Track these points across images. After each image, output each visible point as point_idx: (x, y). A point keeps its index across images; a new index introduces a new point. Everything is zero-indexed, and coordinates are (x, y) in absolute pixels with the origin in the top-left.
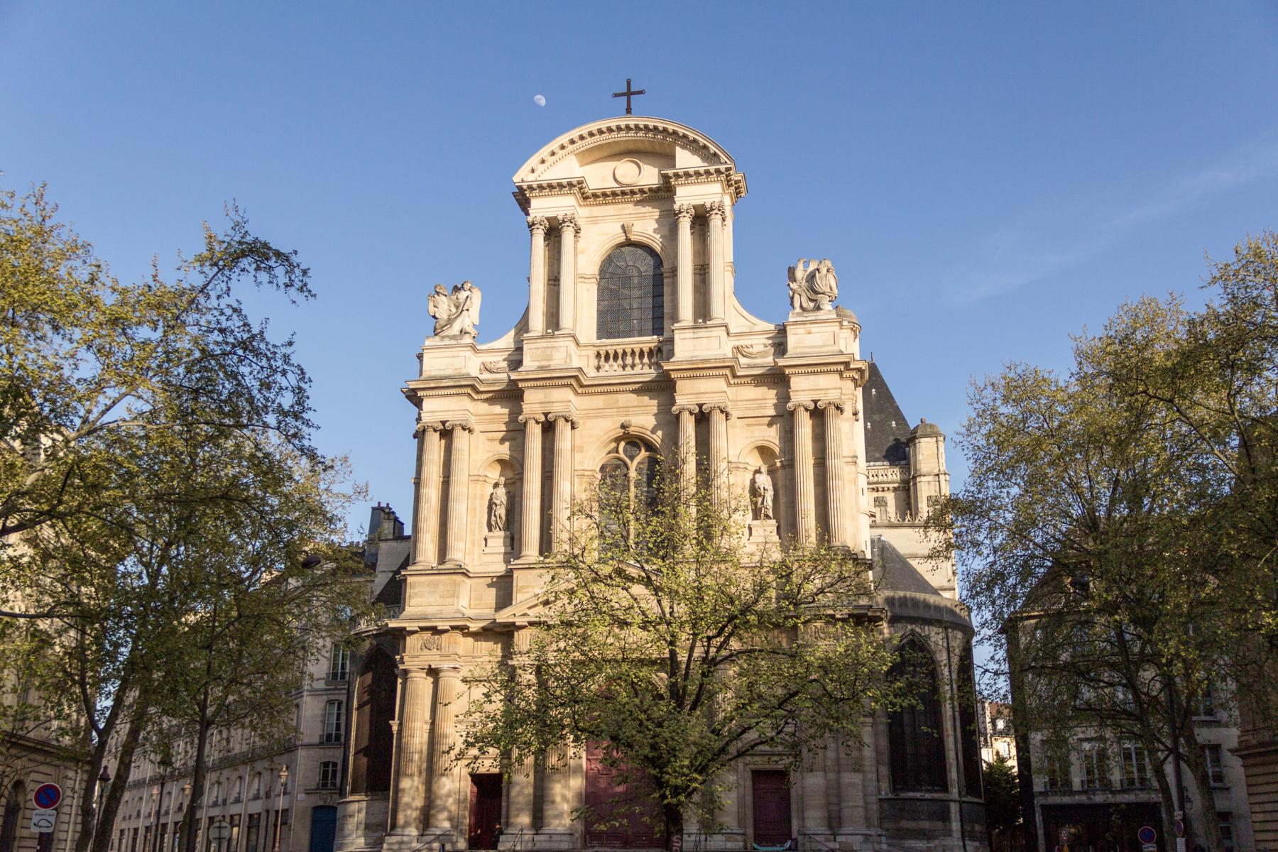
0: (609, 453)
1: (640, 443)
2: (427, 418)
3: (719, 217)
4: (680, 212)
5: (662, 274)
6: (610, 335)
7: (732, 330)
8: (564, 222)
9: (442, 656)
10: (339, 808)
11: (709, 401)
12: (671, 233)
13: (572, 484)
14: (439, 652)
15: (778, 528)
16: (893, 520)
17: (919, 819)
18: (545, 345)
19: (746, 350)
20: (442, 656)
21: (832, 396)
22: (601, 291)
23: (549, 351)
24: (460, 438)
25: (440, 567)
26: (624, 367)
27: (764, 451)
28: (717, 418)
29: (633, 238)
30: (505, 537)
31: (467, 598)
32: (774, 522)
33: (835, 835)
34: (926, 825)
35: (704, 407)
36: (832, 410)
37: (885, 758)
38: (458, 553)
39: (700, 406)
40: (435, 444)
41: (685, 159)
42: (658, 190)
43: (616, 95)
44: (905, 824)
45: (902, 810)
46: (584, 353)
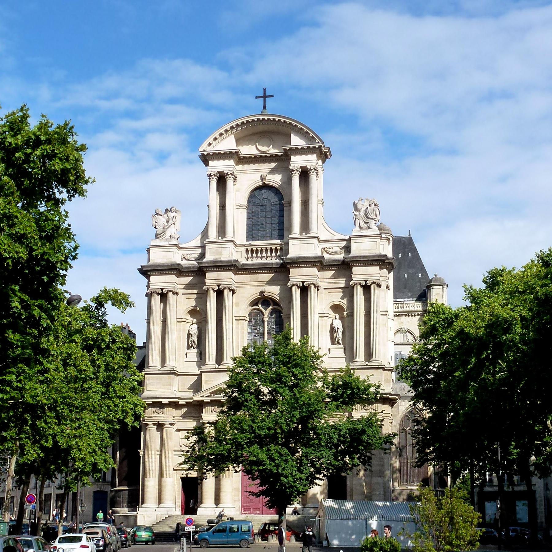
1: (270, 301)
2: (152, 286)
3: (315, 173)
4: (293, 170)
7: (322, 238)
9: (165, 417)
11: (308, 280)
12: (288, 181)
13: (233, 324)
14: (163, 415)
15: (345, 349)
16: (410, 341)
19: (329, 250)
21: (375, 278)
22: (249, 213)
23: (220, 249)
25: (162, 369)
26: (261, 258)
27: (336, 308)
28: (312, 290)
29: (266, 183)
30: (197, 353)
31: (177, 386)
35: (305, 283)
36: (374, 286)
38: (171, 363)
39: (303, 282)
40: (156, 299)
41: (296, 141)
46: (239, 250)
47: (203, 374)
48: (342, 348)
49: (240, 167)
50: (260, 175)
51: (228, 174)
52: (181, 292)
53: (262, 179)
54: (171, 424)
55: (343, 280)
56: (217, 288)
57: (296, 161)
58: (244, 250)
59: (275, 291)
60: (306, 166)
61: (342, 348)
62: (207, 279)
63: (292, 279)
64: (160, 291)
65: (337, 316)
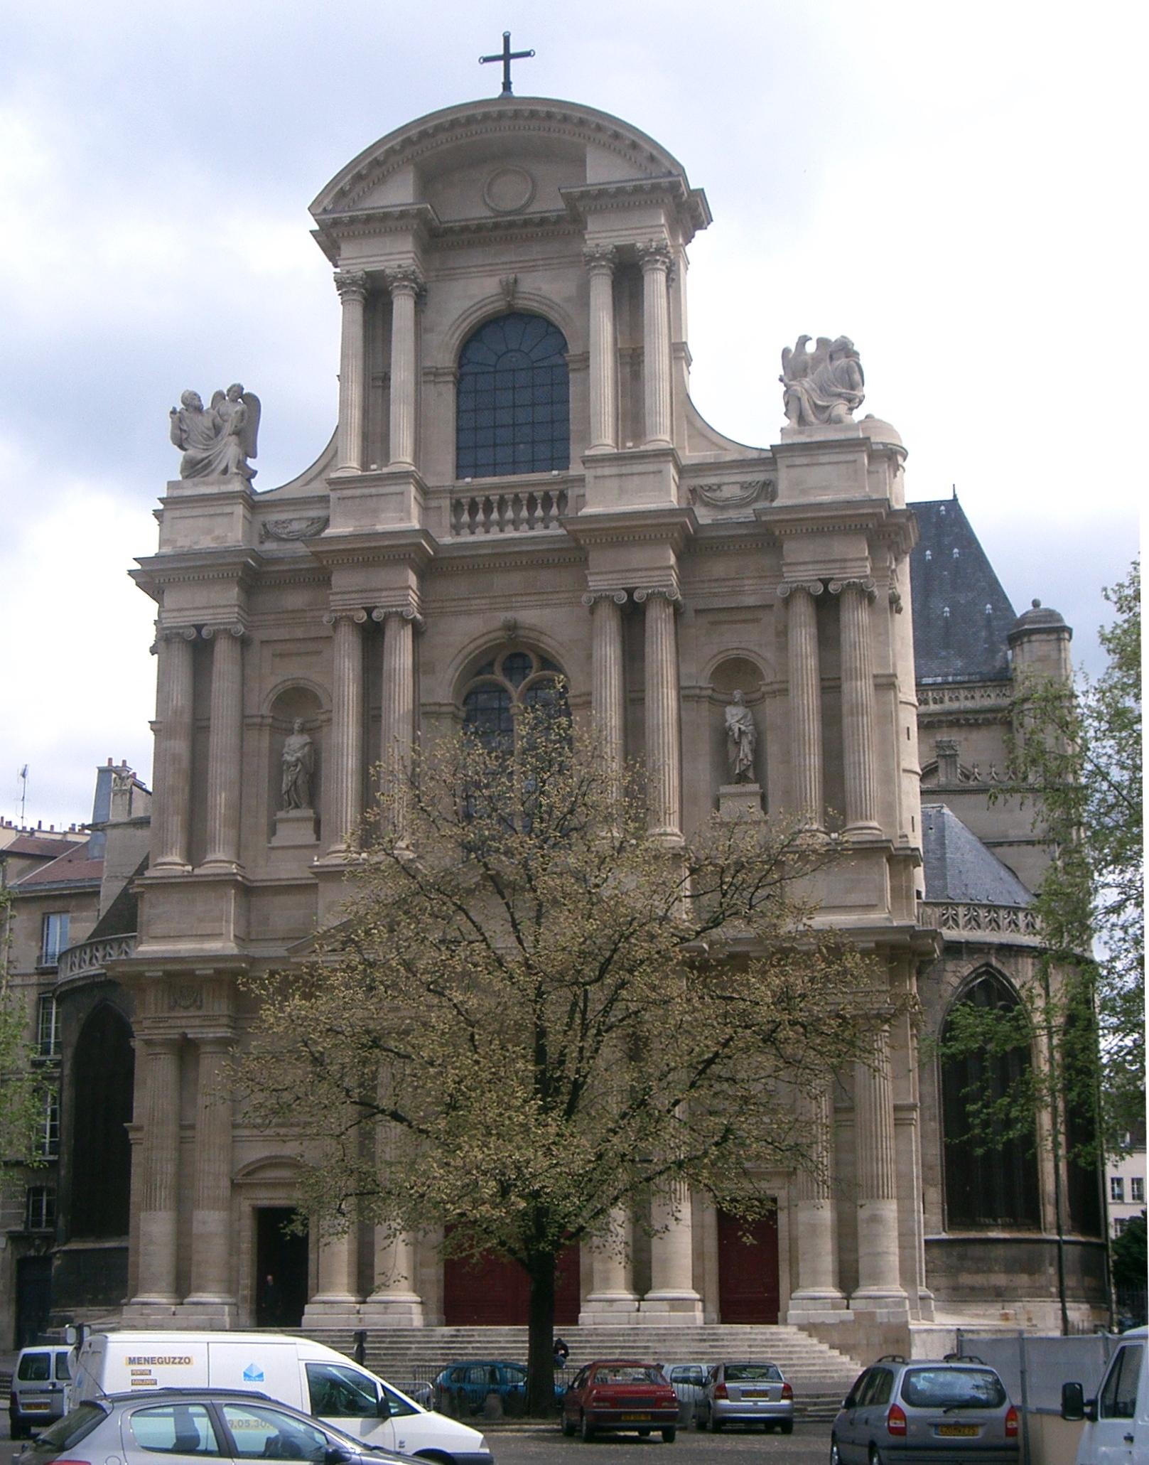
1: (532, 656)
5: (566, 365)
6: (477, 469)
9: (205, 1017)
17: (990, 1271)
18: (366, 491)
20: (205, 1017)
29: (521, 303)
33: (848, 1298)
34: (1000, 1279)
37: (938, 1173)
39: (630, 592)
42: (559, 220)
43: (487, 60)
44: (966, 1279)
45: (962, 1258)
50: (497, 279)
51: (395, 278)
56: (363, 616)
60: (634, 245)
62: (335, 590)
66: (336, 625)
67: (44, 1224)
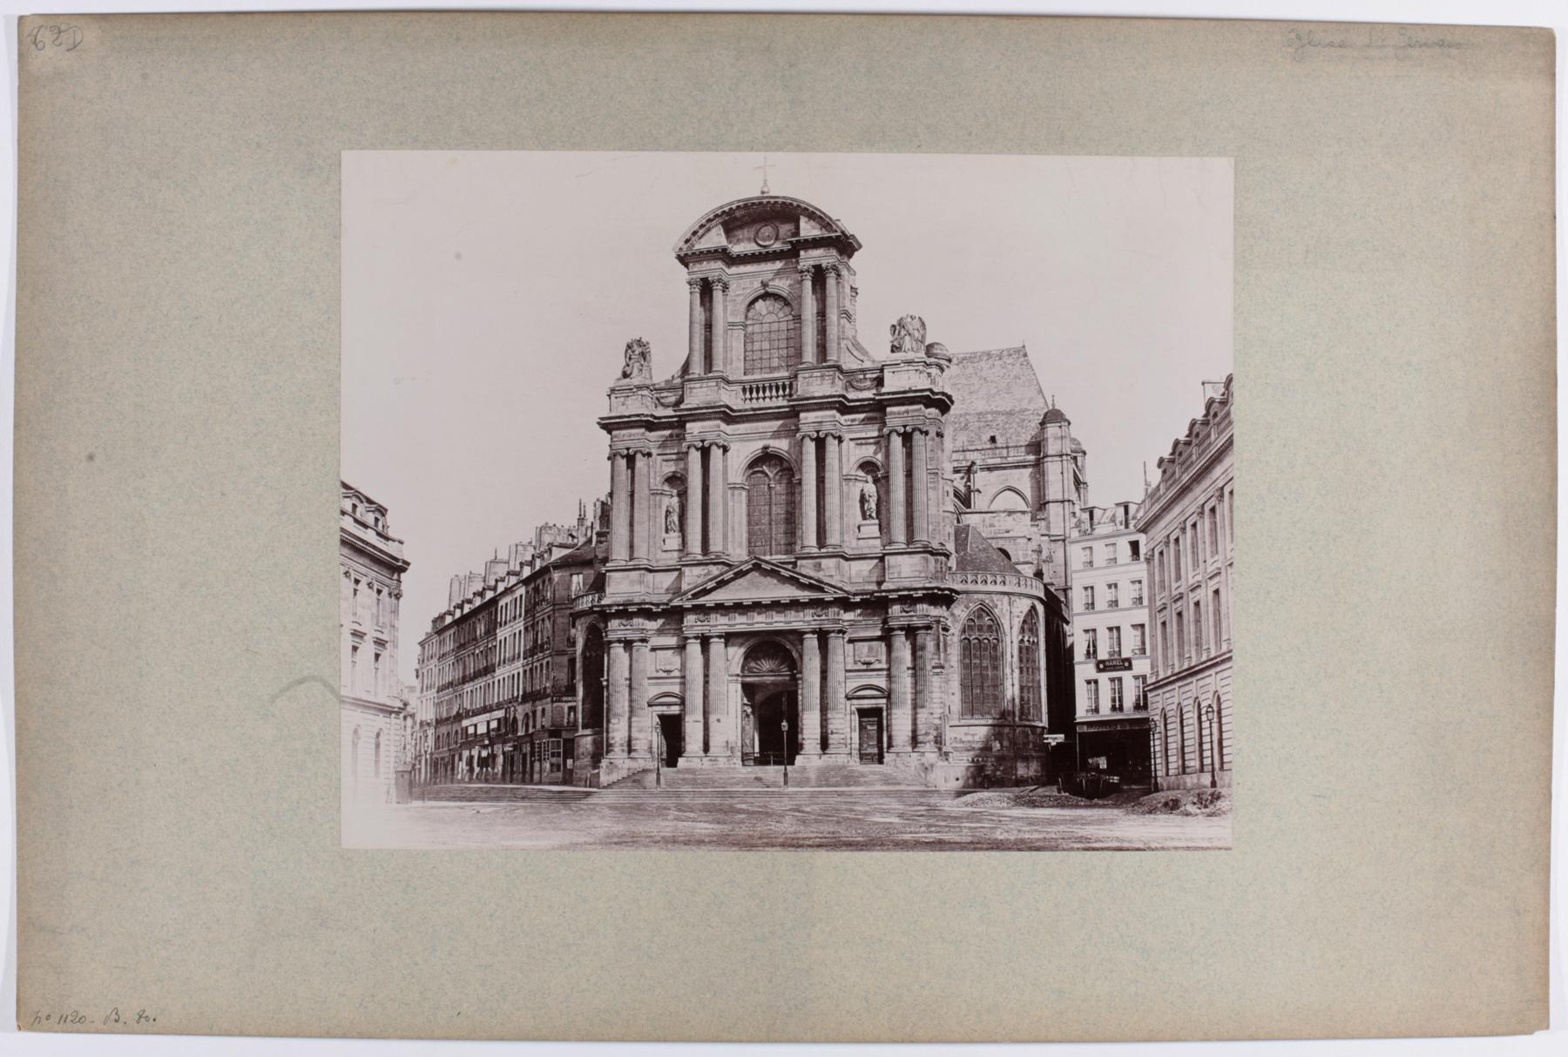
0: (744, 474)
3: (833, 274)
8: (713, 282)
10: (576, 739)
15: (880, 525)
24: (640, 463)
25: (629, 563)
27: (867, 466)
32: (877, 521)
35: (820, 433)
40: (622, 463)
46: (734, 388)
47: (887, 558)
48: (874, 524)
49: (734, 270)
52: (654, 452)
53: (764, 285)
54: (644, 640)
55: (876, 427)
56: (700, 444)
57: (809, 258)
58: (739, 388)
59: (782, 445)
61: (874, 524)
63: (804, 429)
64: (816, 435)
65: (870, 478)
66: (689, 448)
67: (580, 728)
